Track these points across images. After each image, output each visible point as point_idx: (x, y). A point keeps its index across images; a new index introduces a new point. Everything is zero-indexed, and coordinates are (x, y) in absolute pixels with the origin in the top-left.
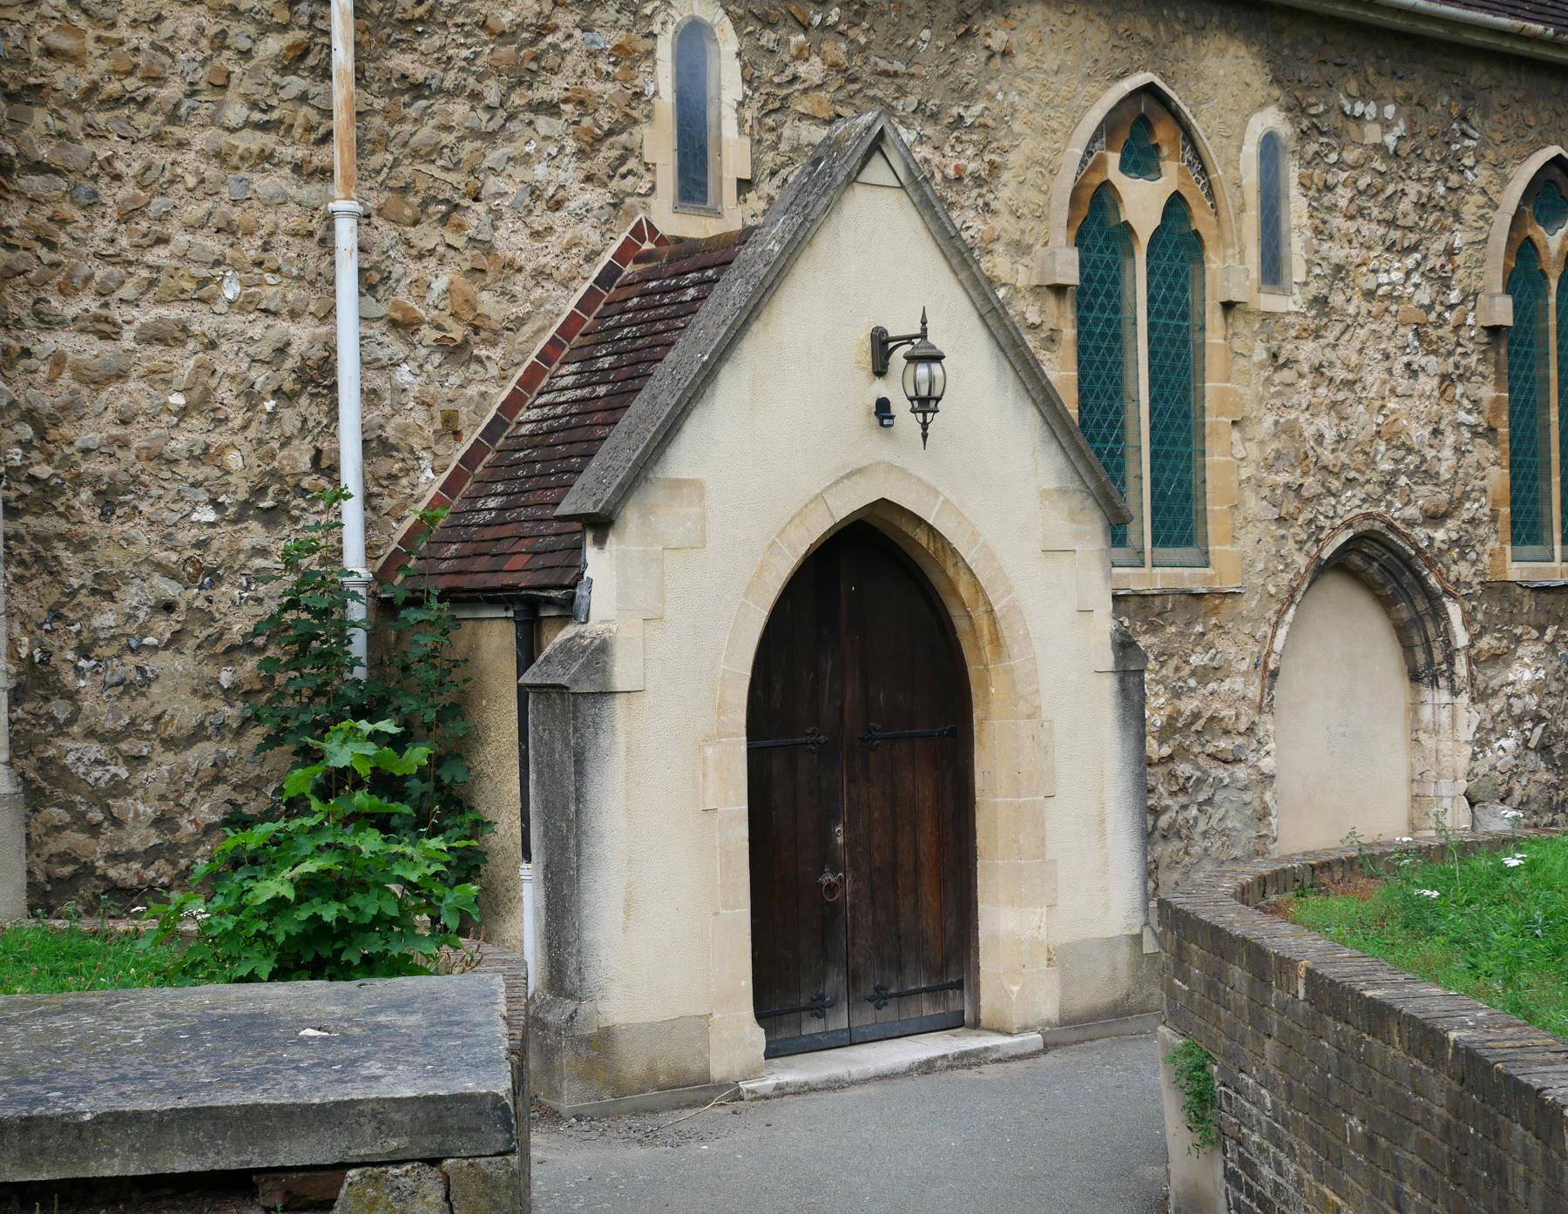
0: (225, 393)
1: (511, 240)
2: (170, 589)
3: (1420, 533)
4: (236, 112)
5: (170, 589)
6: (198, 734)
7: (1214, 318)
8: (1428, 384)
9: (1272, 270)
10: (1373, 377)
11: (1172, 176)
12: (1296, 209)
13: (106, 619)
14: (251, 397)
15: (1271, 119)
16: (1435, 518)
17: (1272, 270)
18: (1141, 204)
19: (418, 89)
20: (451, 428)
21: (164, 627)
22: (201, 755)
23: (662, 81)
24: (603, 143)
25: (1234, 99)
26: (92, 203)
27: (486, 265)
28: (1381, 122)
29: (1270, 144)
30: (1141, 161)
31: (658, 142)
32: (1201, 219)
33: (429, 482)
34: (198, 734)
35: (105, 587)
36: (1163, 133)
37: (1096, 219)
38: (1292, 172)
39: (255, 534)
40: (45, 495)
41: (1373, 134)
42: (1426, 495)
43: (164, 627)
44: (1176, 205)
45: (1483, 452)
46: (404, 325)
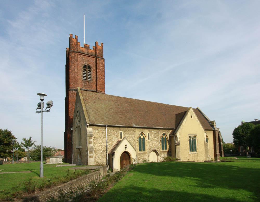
0: (102, 147)
1: (113, 141)
2: (100, 154)
3: (157, 150)
4: (103, 137)
5: (100, 154)
6: (101, 159)
7: (146, 141)
8: (157, 143)
9: (149, 139)
10: (154, 143)
11: (143, 135)
12: (150, 136)
13: (98, 155)
14: (103, 147)
15: (149, 133)
16: (158, 149)
17: (149, 139)
18: (142, 137)
19: (110, 136)
20: (111, 148)
21: (100, 155)
22: (101, 160)
23: (120, 134)
24: (117, 137)
25: (146, 132)
26: (97, 141)
27: (112, 142)
28: (154, 132)
29: (149, 134)
30: (142, 135)
31: (120, 137)
32: (145, 137)
33: (110, 150)
34: (101, 159)
35: (98, 154)
36: (143, 134)
37: (140, 138)
38: (150, 135)
39: (103, 152)
40: (96, 151)
41: (154, 133)
42: (157, 148)
43: (100, 155)
44: (144, 137)
45: (160, 146)
46: (109, 144)
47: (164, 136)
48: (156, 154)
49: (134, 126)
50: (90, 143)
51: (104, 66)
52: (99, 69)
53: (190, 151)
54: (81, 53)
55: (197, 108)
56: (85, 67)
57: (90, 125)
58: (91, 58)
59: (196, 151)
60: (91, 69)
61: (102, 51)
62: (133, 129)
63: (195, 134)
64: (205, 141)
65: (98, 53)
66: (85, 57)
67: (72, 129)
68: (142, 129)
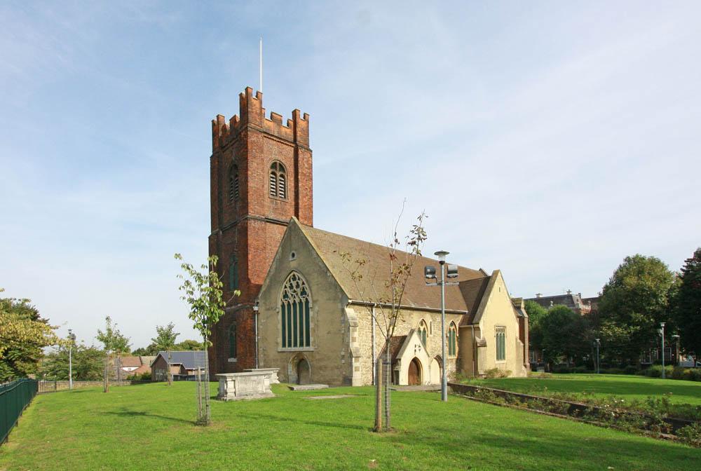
9: (431, 333)
11: (424, 326)
17: (431, 333)
25: (428, 317)
47: (452, 328)
48: (439, 364)
49: (413, 306)
50: (354, 340)
51: (310, 167)
52: (302, 173)
53: (498, 359)
54: (268, 134)
55: (480, 270)
56: (274, 166)
57: (353, 304)
58: (285, 146)
59: (504, 358)
60: (284, 172)
61: (306, 132)
62: (409, 311)
63: (504, 325)
64: (516, 339)
65: (300, 136)
66: (275, 142)
67: (256, 308)
68: (422, 313)
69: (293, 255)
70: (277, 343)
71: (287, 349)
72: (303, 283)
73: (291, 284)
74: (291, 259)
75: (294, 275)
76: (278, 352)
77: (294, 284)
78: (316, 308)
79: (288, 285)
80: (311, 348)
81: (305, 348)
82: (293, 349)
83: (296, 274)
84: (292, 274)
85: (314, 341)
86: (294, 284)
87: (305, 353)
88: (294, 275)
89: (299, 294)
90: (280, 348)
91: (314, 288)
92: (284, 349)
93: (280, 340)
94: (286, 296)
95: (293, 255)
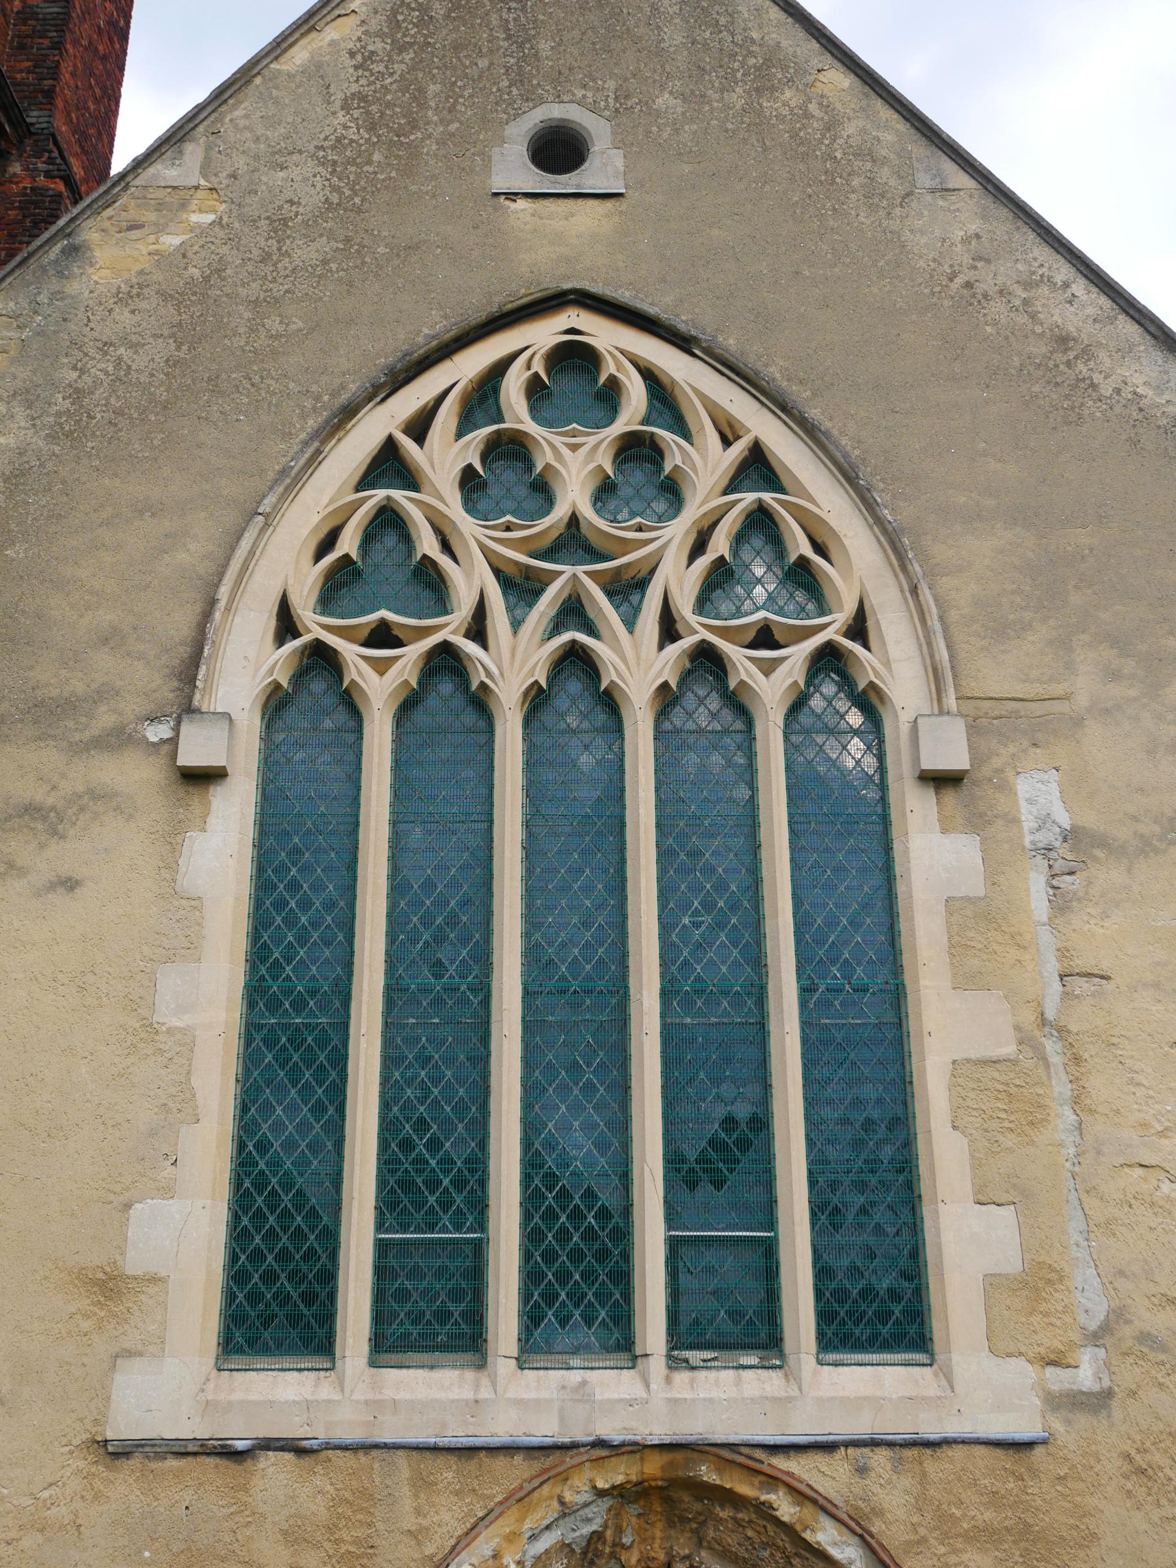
69: (559, 150)
70: (110, 1287)
71: (354, 1392)
72: (757, 467)
73: (509, 449)
74: (513, 168)
75: (574, 357)
76: (117, 1453)
77: (576, 463)
78: (1038, 796)
79: (445, 457)
80: (976, 1384)
81: (812, 1394)
82: (517, 1395)
83: (604, 335)
84: (543, 334)
85: (1032, 1286)
86: (576, 463)
87: (826, 1476)
88: (574, 357)
89: (678, 580)
90: (177, 1381)
91: (975, 559)
92: (280, 1395)
93: (186, 1233)
94: (378, 566)
95: (559, 150)
